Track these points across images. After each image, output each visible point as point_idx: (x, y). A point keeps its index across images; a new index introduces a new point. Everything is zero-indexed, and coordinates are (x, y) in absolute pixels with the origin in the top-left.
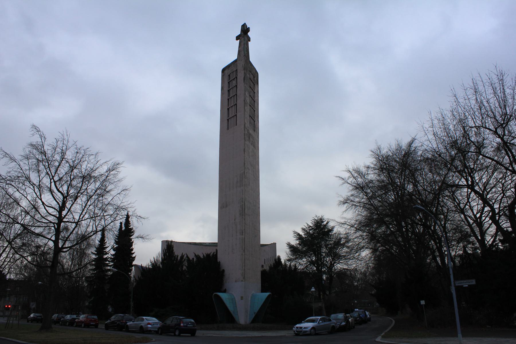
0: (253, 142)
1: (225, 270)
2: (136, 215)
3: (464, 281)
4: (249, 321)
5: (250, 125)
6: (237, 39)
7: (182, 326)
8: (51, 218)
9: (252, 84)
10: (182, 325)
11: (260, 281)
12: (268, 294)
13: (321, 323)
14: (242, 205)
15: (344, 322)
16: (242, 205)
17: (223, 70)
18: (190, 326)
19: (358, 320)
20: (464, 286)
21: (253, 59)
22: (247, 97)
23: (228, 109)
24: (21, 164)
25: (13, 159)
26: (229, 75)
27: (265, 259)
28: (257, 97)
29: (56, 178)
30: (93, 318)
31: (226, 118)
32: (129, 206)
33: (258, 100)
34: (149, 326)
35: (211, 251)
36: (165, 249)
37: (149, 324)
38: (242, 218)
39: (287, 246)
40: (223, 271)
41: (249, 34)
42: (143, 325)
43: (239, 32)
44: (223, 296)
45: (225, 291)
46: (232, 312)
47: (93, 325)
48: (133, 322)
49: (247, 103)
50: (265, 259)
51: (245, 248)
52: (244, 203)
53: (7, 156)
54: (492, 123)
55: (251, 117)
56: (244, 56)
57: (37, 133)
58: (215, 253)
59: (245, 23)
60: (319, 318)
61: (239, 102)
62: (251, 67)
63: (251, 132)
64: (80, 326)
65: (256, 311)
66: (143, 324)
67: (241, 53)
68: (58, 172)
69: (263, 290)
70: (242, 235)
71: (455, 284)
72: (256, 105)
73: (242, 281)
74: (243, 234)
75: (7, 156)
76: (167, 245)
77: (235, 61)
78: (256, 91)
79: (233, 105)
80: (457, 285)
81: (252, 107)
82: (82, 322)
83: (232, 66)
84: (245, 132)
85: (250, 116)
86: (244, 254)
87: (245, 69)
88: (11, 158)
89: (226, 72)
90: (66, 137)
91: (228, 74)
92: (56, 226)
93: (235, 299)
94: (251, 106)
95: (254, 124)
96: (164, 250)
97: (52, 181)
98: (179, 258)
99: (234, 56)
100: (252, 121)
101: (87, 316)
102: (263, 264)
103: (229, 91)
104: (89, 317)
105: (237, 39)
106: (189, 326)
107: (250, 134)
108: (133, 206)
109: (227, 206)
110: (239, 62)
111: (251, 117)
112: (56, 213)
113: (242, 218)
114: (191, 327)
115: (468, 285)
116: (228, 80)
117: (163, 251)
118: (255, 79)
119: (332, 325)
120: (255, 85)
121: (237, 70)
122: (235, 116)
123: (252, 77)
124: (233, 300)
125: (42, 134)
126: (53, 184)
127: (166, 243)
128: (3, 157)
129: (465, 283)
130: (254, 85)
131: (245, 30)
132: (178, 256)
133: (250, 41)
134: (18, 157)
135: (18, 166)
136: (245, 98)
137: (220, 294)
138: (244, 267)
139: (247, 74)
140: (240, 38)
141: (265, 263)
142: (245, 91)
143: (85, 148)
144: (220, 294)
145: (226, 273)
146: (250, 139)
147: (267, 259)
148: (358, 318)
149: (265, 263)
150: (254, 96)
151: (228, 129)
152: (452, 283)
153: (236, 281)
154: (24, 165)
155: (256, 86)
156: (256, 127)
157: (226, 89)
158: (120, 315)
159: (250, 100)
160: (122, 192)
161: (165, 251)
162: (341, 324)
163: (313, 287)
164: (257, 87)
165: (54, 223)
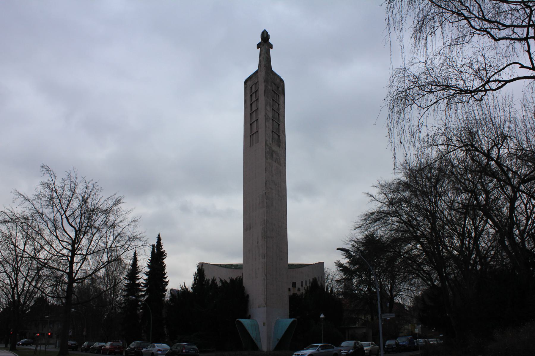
0: (277, 159)
1: (249, 295)
2: (148, 244)
3: (388, 315)
4: (272, 348)
5: (273, 141)
6: (258, 48)
7: (184, 352)
8: (65, 252)
9: (275, 95)
10: (184, 351)
11: (287, 307)
12: (293, 319)
13: (320, 350)
14: (264, 227)
15: (353, 350)
16: (264, 227)
17: (246, 82)
18: (192, 352)
19: (394, 348)
20: (387, 319)
21: (275, 67)
22: (268, 111)
23: (251, 124)
24: (34, 202)
25: (26, 199)
26: (251, 87)
27: (302, 282)
28: (283, 108)
29: (68, 213)
30: (118, 346)
31: (249, 134)
32: (141, 236)
33: (284, 111)
34: (159, 352)
35: (234, 275)
36: (195, 273)
37: (159, 350)
38: (264, 241)
39: (336, 265)
40: (248, 296)
41: (270, 41)
42: (154, 351)
43: (259, 40)
44: (245, 322)
45: (249, 317)
46: (254, 339)
47: (118, 352)
48: (147, 348)
49: (269, 118)
50: (302, 282)
51: (266, 272)
52: (265, 226)
53: (22, 196)
54: (532, 128)
55: (274, 132)
56: (264, 66)
57: (47, 172)
58: (241, 278)
59: (265, 30)
60: (320, 345)
61: (260, 117)
62: (273, 77)
63: (275, 148)
64: (106, 354)
65: (280, 338)
66: (154, 350)
67: (261, 63)
68: (71, 205)
69: (290, 317)
70: (264, 259)
71: (381, 317)
72: (281, 117)
73: (264, 307)
74: (265, 258)
75: (22, 196)
76: (197, 269)
77: (256, 72)
78: (281, 103)
79: (255, 120)
80: (383, 317)
81: (275, 122)
82: (107, 349)
83: (254, 77)
84: (266, 150)
85: (273, 131)
86: (266, 278)
87: (266, 81)
88: (25, 198)
89: (248, 83)
90: (73, 175)
91: (250, 86)
92: (70, 259)
93: (258, 325)
94: (274, 121)
95: (279, 139)
96: (195, 275)
97: (64, 216)
98: (210, 282)
99: (253, 67)
100: (276, 136)
101: (112, 343)
102: (300, 287)
103: (251, 104)
104: (115, 344)
105: (258, 48)
106: (191, 352)
107: (273, 151)
108: (144, 236)
109: (250, 228)
110: (259, 73)
111: (274, 132)
112: (70, 247)
113: (264, 241)
114: (193, 353)
115: (390, 318)
116: (250, 93)
117: (194, 275)
118: (280, 89)
119: (335, 352)
120: (280, 96)
121: (258, 82)
122: (257, 133)
123: (275, 87)
124: (256, 327)
125: (52, 173)
126: (65, 220)
127: (197, 267)
128: (18, 197)
129: (388, 316)
130: (278, 96)
131: (265, 36)
132: (209, 280)
133: (272, 48)
134: (31, 197)
135: (31, 205)
136: (266, 113)
137: (243, 321)
138: (266, 292)
139: (268, 86)
140: (261, 46)
141: (302, 286)
142: (266, 105)
143: (93, 182)
144: (243, 321)
145: (251, 298)
146: (272, 156)
147: (306, 281)
148: (394, 345)
149: (302, 286)
150: (278, 109)
151: (251, 146)
152: (379, 316)
153: (259, 307)
154: (37, 203)
155: (281, 97)
156: (281, 142)
157: (249, 103)
158: (138, 343)
159: (272, 114)
160: (131, 224)
161: (196, 276)
162: (348, 351)
163: (322, 314)
164: (283, 97)
165: (67, 256)
